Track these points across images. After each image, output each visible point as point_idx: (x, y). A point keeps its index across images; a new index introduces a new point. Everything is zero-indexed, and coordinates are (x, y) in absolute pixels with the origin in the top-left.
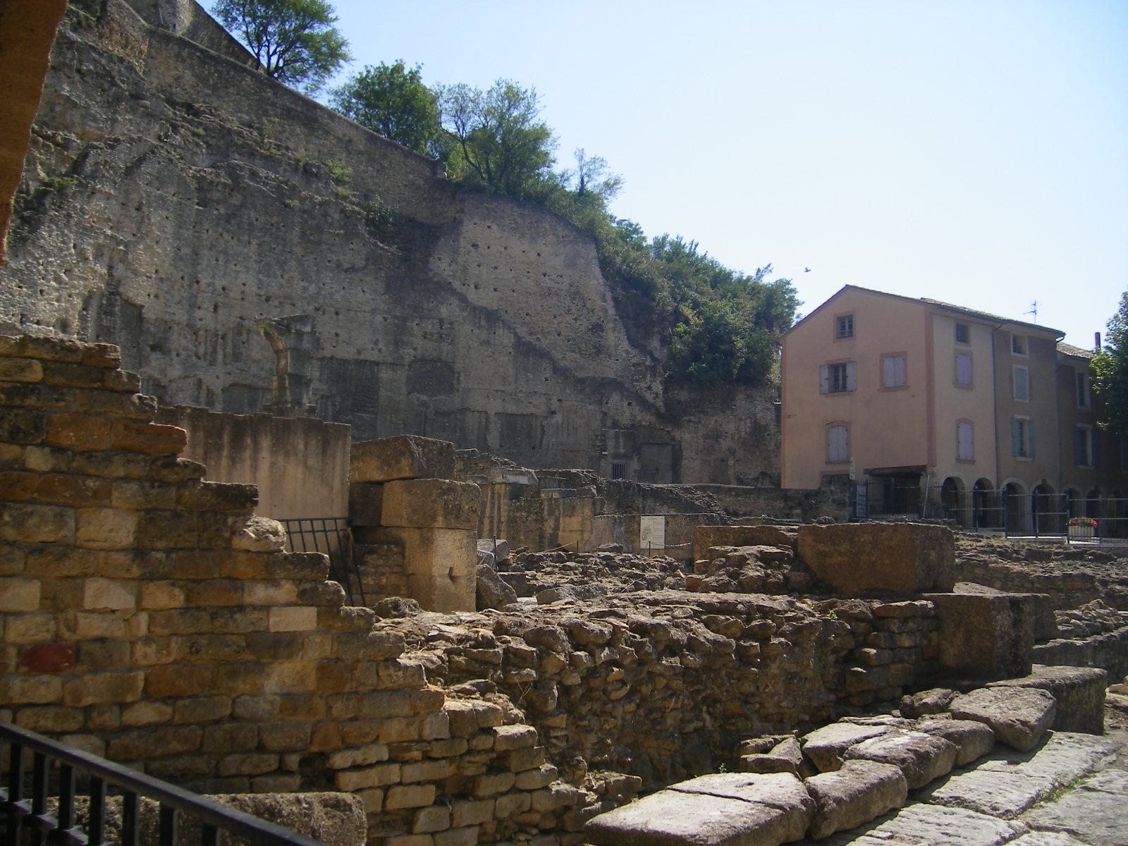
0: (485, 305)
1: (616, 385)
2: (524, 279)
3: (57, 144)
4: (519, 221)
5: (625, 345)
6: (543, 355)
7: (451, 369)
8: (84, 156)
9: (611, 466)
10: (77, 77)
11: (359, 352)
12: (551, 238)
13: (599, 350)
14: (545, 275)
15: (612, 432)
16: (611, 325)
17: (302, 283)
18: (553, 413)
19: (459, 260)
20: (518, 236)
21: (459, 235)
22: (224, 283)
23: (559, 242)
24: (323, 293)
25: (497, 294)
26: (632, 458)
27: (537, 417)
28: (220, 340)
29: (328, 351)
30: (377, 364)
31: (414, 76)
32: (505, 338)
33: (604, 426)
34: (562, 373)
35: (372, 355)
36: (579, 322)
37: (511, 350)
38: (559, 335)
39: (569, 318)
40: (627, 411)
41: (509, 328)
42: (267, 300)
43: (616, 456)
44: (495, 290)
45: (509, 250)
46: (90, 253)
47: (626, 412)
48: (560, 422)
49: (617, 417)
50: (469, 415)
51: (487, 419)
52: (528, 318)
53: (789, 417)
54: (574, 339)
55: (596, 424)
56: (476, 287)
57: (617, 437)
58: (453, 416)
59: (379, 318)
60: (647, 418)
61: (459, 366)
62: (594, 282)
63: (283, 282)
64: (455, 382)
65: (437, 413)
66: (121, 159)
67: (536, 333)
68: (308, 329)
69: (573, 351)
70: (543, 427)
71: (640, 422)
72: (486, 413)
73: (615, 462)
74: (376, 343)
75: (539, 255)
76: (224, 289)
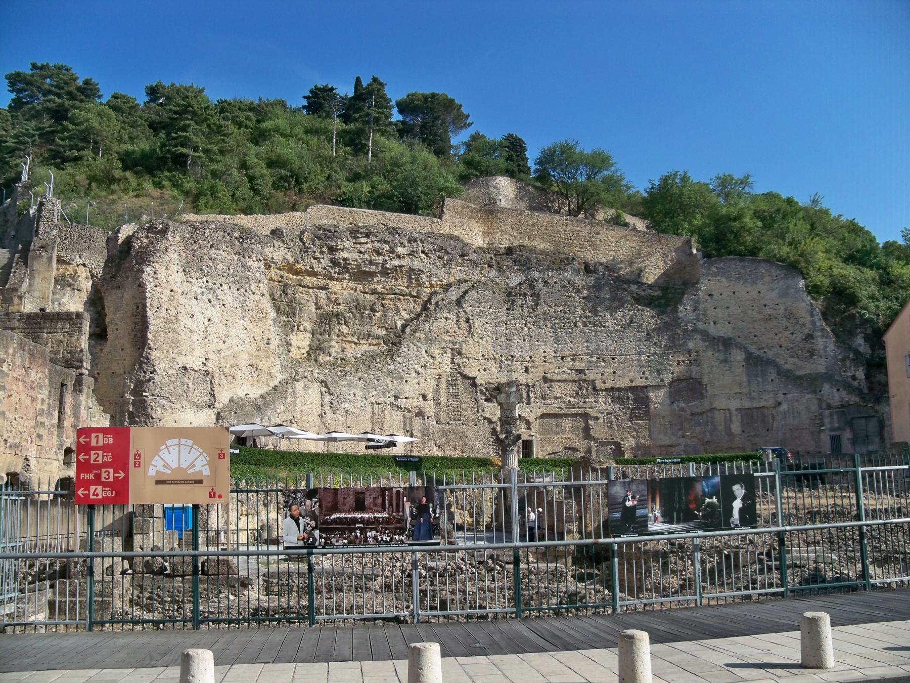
0: (722, 335)
1: (828, 377)
2: (750, 312)
3: (415, 297)
4: (742, 271)
5: (831, 347)
6: (771, 363)
7: (700, 383)
8: (429, 300)
9: (829, 437)
10: (423, 256)
11: (632, 381)
12: (767, 279)
13: (812, 353)
14: (765, 306)
15: (827, 412)
16: (819, 334)
17: (586, 344)
18: (780, 404)
19: (700, 307)
20: (742, 282)
21: (697, 291)
22: (531, 354)
23: (773, 280)
24: (601, 347)
25: (730, 325)
26: (845, 430)
27: (767, 408)
28: (531, 389)
29: (609, 384)
30: (646, 387)
31: (684, 179)
32: (738, 356)
33: (820, 408)
34: (788, 376)
35: (639, 382)
36: (795, 335)
37: (744, 364)
38: (781, 347)
39: (787, 333)
40: (837, 395)
41: (740, 348)
42: (562, 358)
43: (832, 429)
44: (729, 323)
45: (736, 293)
46: (436, 352)
47: (834, 395)
48: (786, 409)
49: (828, 401)
50: (717, 413)
51: (730, 414)
52: (756, 338)
53: (893, 397)
54: (792, 348)
55: (814, 408)
56: (715, 323)
57: (831, 415)
58: (705, 415)
59: (644, 358)
60: (854, 399)
61: (705, 380)
62: (804, 304)
63: (572, 346)
64: (704, 391)
65: (692, 414)
66: (454, 295)
67: (763, 348)
68: (514, 389)
69: (792, 357)
70: (773, 414)
71: (847, 402)
72: (729, 410)
73: (832, 434)
74: (644, 373)
75: (759, 292)
76: (531, 357)
